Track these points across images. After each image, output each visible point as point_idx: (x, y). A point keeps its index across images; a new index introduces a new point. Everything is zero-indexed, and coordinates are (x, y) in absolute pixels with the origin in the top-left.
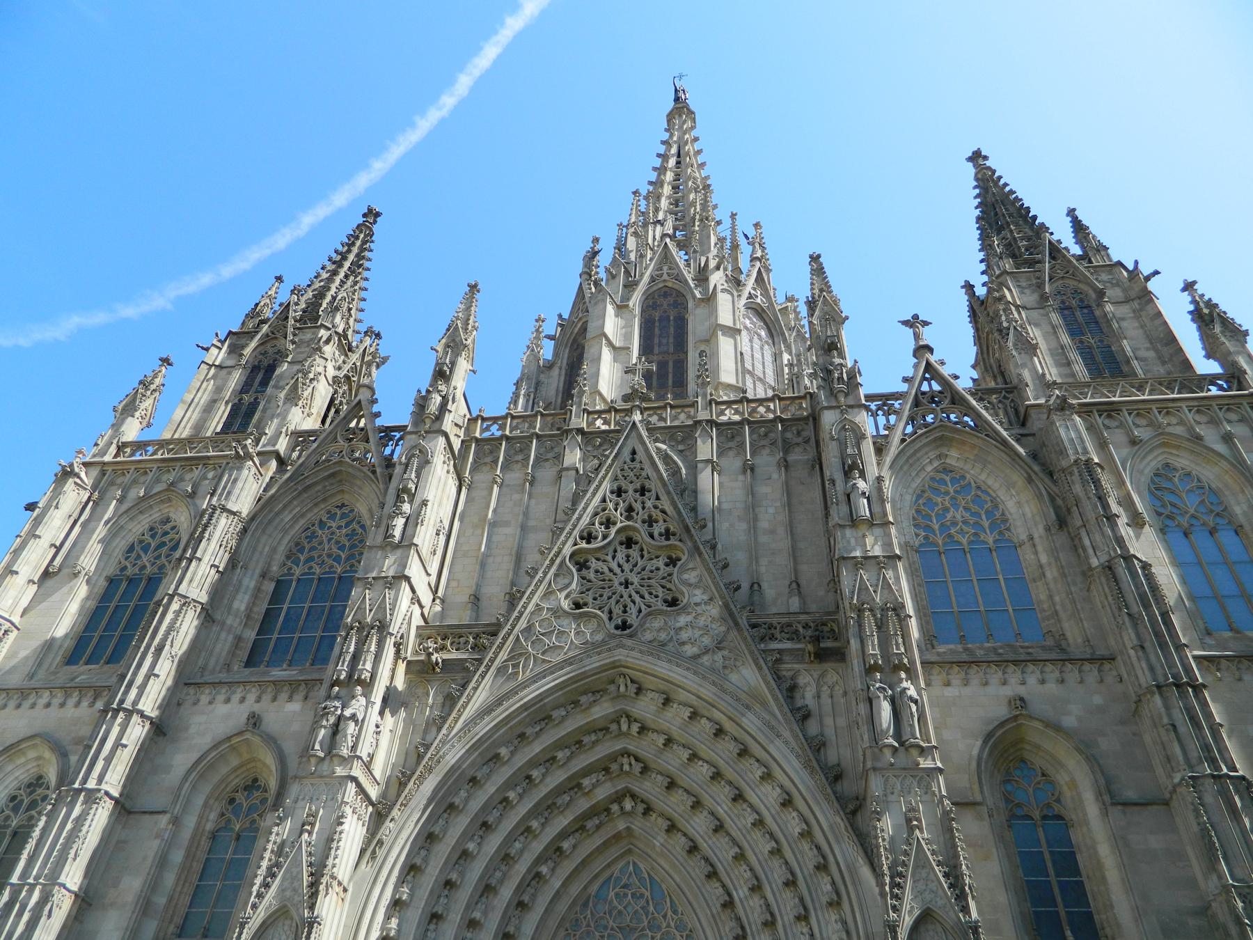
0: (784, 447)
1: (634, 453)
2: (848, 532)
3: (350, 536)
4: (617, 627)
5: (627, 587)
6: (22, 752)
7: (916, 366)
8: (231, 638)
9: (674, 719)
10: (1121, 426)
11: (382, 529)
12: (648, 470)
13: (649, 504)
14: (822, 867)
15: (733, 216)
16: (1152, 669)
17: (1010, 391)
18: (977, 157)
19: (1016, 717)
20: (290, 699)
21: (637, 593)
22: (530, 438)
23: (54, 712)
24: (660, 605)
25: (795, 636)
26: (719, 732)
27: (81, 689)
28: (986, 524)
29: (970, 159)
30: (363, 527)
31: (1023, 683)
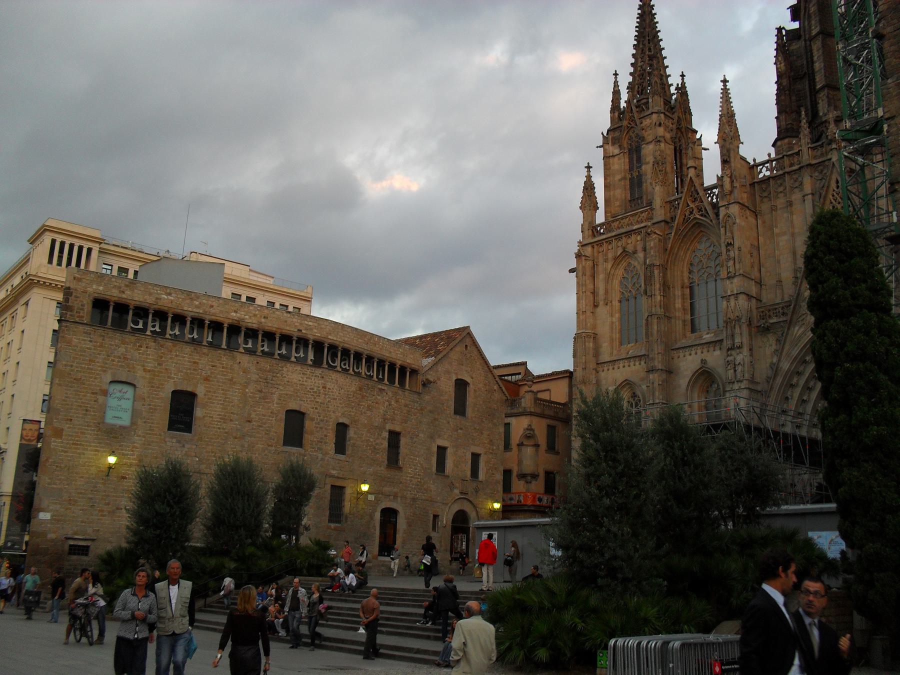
1: (837, 182)
11: (725, 268)
22: (784, 174)
23: (627, 368)
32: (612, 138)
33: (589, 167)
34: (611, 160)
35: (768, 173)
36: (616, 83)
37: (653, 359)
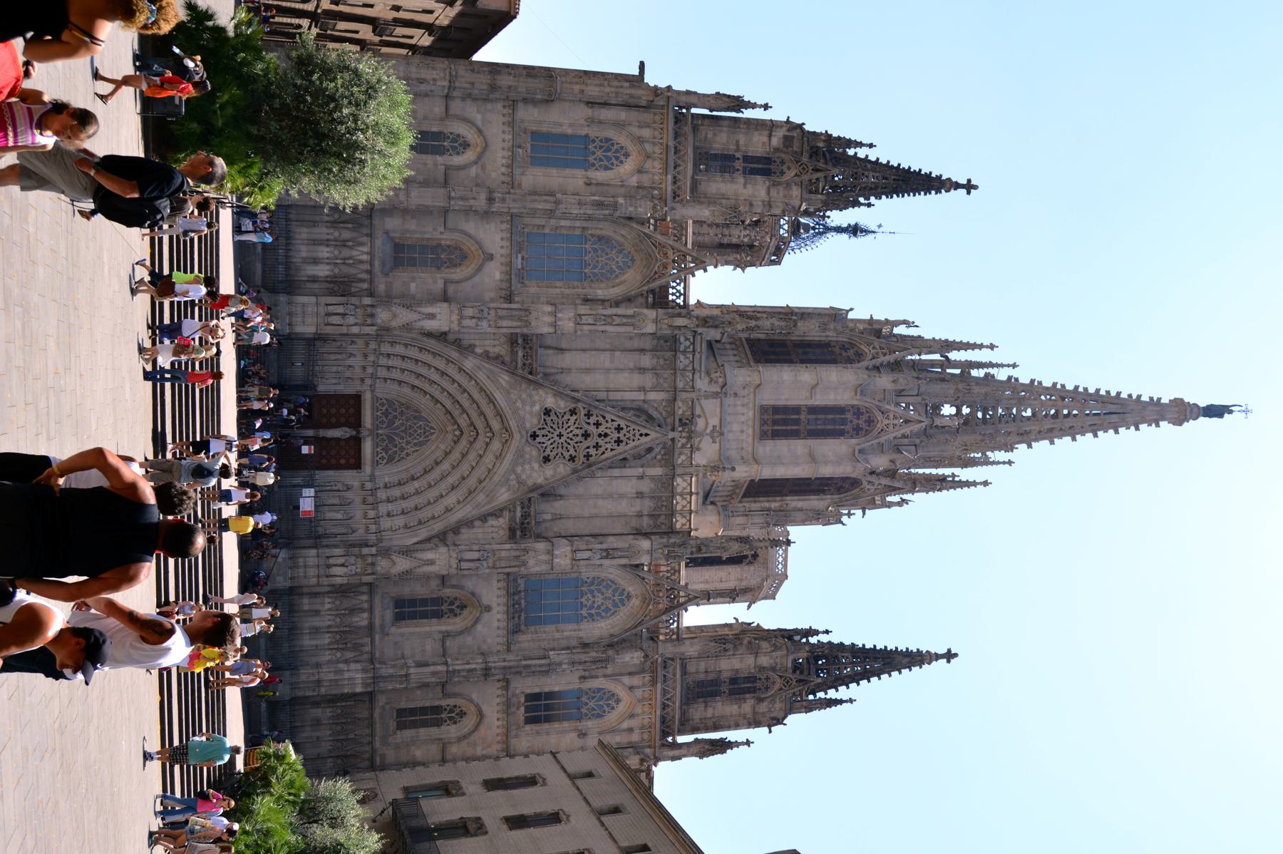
1: (647, 435)
2: (569, 548)
3: (612, 271)
9: (489, 459)
10: (644, 685)
11: (588, 312)
12: (632, 444)
13: (609, 446)
14: (420, 523)
15: (1010, 463)
18: (949, 656)
25: (525, 516)
26: (480, 482)
27: (513, 157)
28: (593, 611)
29: (949, 650)
32: (793, 137)
33: (766, 107)
34: (766, 133)
35: (682, 348)
36: (860, 145)
37: (503, 200)
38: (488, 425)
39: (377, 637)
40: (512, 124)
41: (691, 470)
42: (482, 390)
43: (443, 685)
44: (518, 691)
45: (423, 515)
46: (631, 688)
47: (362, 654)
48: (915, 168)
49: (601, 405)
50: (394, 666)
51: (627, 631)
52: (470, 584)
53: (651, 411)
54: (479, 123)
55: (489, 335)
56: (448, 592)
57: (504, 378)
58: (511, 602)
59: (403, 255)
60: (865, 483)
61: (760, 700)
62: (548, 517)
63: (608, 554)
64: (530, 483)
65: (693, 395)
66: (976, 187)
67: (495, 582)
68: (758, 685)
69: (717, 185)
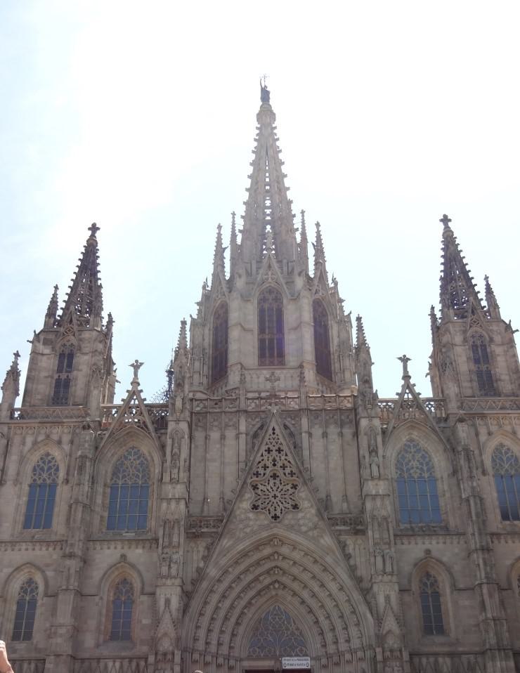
0: (341, 424)
1: (274, 429)
2: (370, 483)
3: (141, 464)
4: (272, 517)
5: (275, 499)
6: (22, 570)
7: (403, 386)
8: (99, 517)
9: (297, 555)
10: (486, 425)
11: (169, 473)
12: (282, 440)
13: (283, 458)
14: (354, 612)
16: (475, 542)
17: (443, 400)
18: (445, 220)
19: (426, 558)
20: (137, 548)
21: (280, 501)
22: (221, 412)
24: (290, 507)
25: (345, 524)
26: (316, 561)
27: (40, 542)
28: (425, 468)
29: (441, 220)
30: (146, 460)
31: (431, 544)
32: (45, 339)
33: (17, 355)
34: (40, 357)
36: (55, 296)
37: (72, 545)
38: (268, 558)
39: (461, 649)
40: (13, 543)
41: (303, 397)
42: (236, 563)
43: (501, 589)
44: (500, 526)
45: (347, 610)
46: (490, 434)
47: (476, 662)
48: (79, 263)
49: (249, 464)
50: (487, 631)
51: (441, 440)
52: (407, 568)
53: (255, 429)
54: (10, 570)
55: (188, 556)
56: (415, 587)
57: (226, 542)
58: (421, 533)
59: (119, 630)
60: (317, 296)
61: (491, 340)
62: (345, 505)
63: (373, 451)
64: (316, 519)
65: (242, 398)
66: (94, 225)
67: (404, 547)
68: (479, 343)
69: (78, 389)
